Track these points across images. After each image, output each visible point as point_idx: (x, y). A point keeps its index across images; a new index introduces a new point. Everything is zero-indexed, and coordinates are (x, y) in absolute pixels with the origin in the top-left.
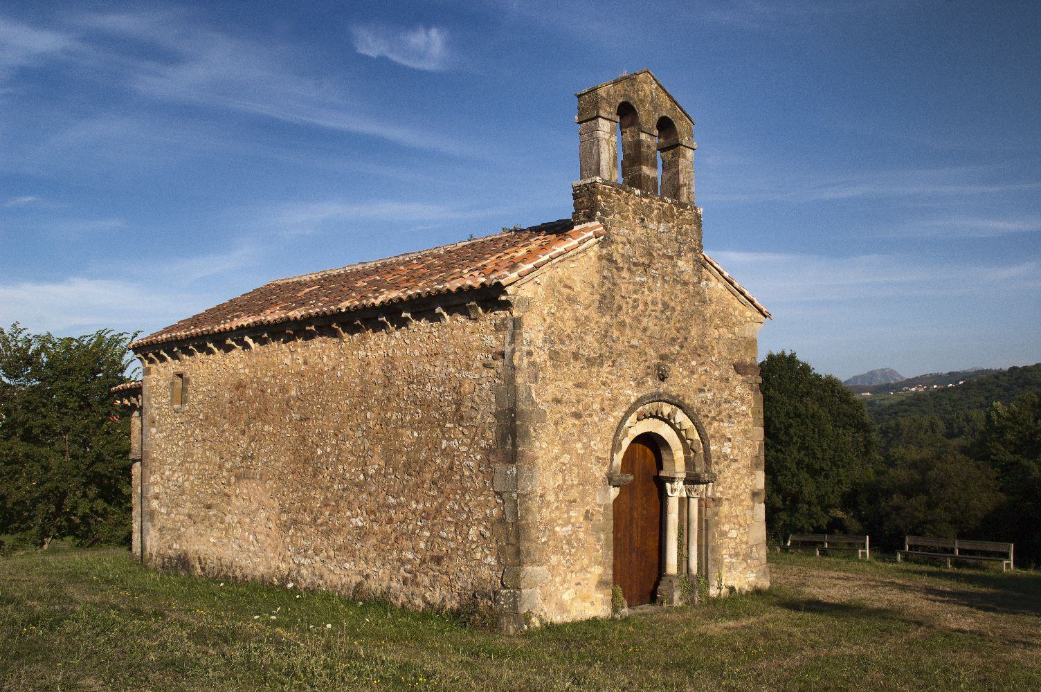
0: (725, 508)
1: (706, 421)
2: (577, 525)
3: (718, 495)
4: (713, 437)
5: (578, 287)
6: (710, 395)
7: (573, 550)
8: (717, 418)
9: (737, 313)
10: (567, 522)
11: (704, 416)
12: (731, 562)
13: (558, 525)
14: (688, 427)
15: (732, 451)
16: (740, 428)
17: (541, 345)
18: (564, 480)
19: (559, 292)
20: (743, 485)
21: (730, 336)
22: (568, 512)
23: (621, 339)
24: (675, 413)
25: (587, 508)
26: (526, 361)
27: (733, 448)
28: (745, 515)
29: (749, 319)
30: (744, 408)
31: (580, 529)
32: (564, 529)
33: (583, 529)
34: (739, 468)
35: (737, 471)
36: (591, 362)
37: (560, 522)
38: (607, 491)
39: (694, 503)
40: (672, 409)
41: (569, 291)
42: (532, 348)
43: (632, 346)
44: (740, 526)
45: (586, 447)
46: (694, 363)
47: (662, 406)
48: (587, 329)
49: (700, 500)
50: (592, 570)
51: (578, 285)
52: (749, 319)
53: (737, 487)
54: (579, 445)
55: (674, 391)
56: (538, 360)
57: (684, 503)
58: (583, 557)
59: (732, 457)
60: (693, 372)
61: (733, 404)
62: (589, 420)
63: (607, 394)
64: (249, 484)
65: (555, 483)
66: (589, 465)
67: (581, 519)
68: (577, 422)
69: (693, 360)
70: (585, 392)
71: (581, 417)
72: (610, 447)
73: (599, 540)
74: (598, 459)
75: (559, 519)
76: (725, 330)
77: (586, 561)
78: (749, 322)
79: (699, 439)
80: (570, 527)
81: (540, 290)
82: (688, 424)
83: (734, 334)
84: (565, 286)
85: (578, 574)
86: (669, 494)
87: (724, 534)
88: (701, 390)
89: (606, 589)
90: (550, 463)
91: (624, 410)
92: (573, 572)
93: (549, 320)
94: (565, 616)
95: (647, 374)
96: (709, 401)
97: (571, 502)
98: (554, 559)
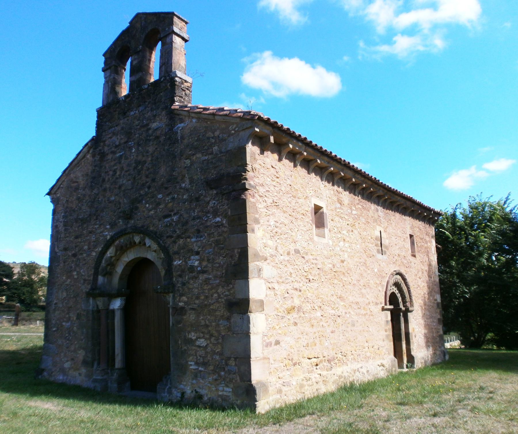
0: (191, 317)
1: (169, 241)
3: (181, 304)
6: (175, 218)
8: (183, 236)
9: (217, 133)
10: (69, 319)
11: (168, 237)
12: (198, 369)
13: (64, 321)
15: (200, 263)
16: (211, 239)
20: (216, 295)
21: (206, 158)
22: (68, 313)
24: (144, 239)
25: (78, 311)
27: (201, 260)
28: (218, 325)
29: (233, 132)
30: (218, 219)
34: (210, 279)
35: (207, 281)
36: (84, 221)
38: (88, 301)
43: (110, 202)
44: (212, 336)
45: (79, 273)
46: (160, 196)
47: (133, 237)
50: (80, 352)
52: (233, 132)
53: (207, 297)
54: (75, 273)
55: (140, 224)
59: (199, 269)
60: (159, 204)
62: (80, 257)
64: (312, 307)
68: (74, 260)
69: (160, 194)
71: (76, 256)
72: (92, 272)
74: (85, 280)
76: (199, 155)
78: (233, 134)
87: (191, 342)
88: (166, 217)
91: (102, 246)
93: (66, 205)
94: (65, 378)
95: (119, 218)
96: (174, 224)
98: (60, 342)
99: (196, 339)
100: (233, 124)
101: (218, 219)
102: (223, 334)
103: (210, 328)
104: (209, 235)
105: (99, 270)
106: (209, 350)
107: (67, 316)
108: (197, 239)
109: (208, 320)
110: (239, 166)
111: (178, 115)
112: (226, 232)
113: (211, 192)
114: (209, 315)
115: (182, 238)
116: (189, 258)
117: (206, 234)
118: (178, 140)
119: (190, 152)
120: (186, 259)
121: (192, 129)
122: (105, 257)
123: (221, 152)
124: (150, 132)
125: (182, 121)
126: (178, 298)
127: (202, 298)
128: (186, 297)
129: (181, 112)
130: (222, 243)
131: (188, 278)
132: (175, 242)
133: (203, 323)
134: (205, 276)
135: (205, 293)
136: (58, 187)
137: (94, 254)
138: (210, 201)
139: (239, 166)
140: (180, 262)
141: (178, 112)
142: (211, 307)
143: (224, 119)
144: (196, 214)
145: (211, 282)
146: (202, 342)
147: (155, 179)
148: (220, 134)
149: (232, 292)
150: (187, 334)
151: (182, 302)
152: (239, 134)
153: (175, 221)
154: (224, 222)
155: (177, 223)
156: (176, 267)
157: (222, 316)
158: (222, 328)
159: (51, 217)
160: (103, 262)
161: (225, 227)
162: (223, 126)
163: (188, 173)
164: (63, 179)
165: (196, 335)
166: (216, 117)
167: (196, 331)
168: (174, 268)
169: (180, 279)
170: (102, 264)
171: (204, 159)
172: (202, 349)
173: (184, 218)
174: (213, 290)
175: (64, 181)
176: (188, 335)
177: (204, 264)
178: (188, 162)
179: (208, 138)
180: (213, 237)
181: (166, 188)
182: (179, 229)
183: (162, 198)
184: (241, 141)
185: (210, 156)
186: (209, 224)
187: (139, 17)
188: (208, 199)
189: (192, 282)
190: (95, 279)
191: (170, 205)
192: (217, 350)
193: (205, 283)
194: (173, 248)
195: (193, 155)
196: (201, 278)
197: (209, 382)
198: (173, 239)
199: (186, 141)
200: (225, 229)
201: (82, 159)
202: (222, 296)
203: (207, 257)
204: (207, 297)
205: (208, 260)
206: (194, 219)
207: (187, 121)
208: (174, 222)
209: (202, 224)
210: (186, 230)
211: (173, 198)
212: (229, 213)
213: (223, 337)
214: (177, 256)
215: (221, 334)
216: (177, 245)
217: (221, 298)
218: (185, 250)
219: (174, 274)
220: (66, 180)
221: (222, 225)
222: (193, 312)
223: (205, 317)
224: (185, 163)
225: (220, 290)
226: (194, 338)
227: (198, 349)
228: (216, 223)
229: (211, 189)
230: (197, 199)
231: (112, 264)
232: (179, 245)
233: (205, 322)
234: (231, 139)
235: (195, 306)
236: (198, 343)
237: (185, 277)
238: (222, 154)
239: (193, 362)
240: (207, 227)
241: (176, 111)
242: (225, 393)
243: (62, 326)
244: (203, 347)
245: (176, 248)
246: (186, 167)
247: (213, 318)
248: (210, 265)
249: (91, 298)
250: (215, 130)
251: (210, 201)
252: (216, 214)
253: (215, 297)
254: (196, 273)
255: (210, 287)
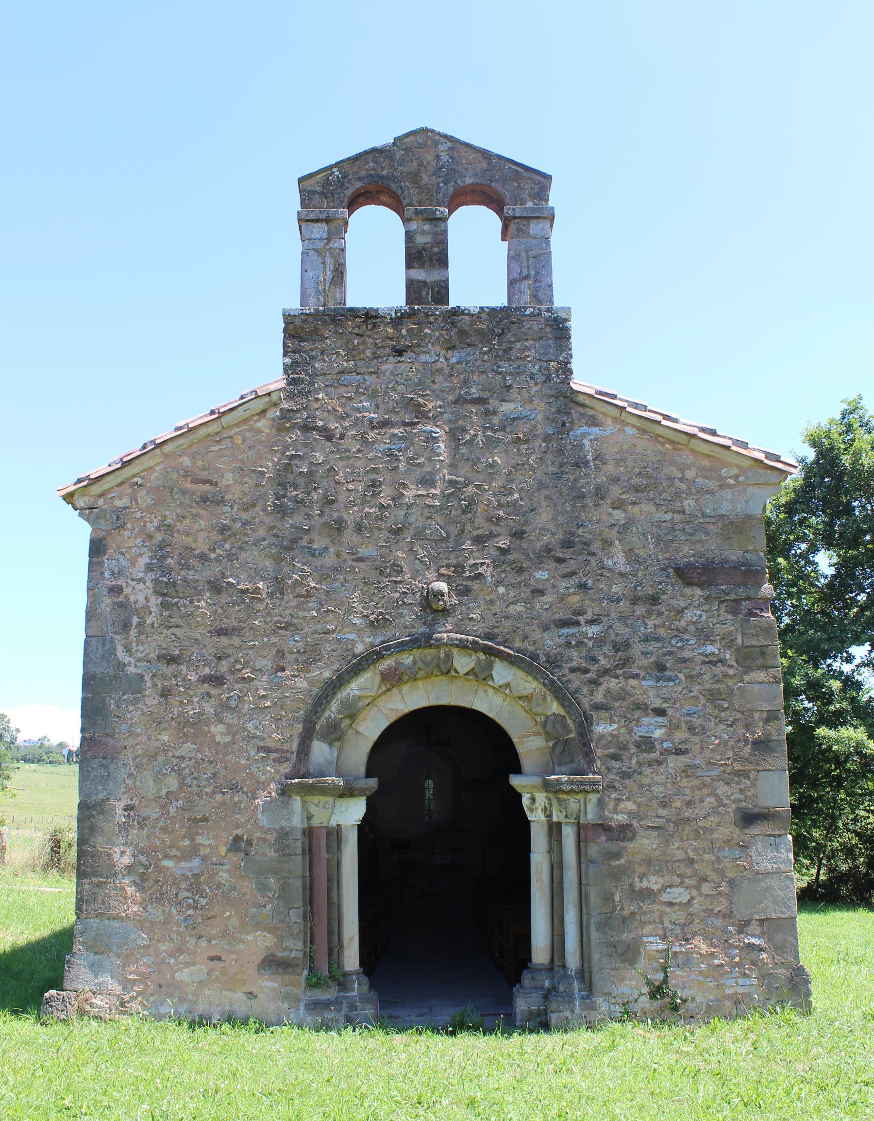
1: (576, 681)
2: (214, 859)
3: (621, 818)
4: (597, 707)
5: (229, 478)
6: (593, 630)
7: (203, 902)
8: (619, 672)
10: (193, 851)
11: (573, 670)
13: (167, 856)
14: (525, 693)
15: (669, 734)
17: (142, 575)
18: (182, 784)
19: (184, 492)
21: (669, 517)
23: (331, 550)
24: (490, 666)
25: (239, 832)
26: (107, 601)
29: (732, 482)
30: (710, 649)
31: (221, 867)
32: (183, 864)
33: (227, 867)
35: (688, 771)
37: (174, 852)
39: (569, 834)
40: (478, 658)
41: (208, 487)
42: (120, 582)
43: (360, 560)
45: (232, 731)
46: (541, 575)
48: (246, 542)
49: (580, 828)
50: (250, 938)
51: (228, 476)
52: (732, 482)
56: (132, 598)
57: (554, 830)
58: (228, 914)
59: (665, 745)
60: (539, 592)
61: (673, 642)
63: (292, 643)
65: (159, 790)
66: (243, 762)
67: (223, 850)
70: (236, 641)
73: (263, 888)
75: (171, 847)
77: (235, 921)
78: (730, 486)
79: (562, 712)
80: (196, 862)
81: (142, 493)
82: (529, 685)
83: (683, 512)
84: (196, 481)
85: (213, 942)
86: (529, 819)
87: (647, 895)
89: (285, 974)
90: (152, 757)
92: (200, 937)
93: (159, 537)
97: (196, 821)
99: (664, 888)
100: (728, 465)
101: (710, 649)
102: (730, 875)
103: (696, 866)
104: (690, 677)
105: (318, 727)
106: (696, 906)
107: (187, 843)
108: (657, 682)
109: (695, 849)
110: (747, 552)
111: (583, 406)
112: (731, 677)
113: (688, 591)
114: (695, 840)
115: (617, 677)
116: (638, 720)
117: (681, 676)
118: (587, 462)
119: (624, 497)
120: (629, 722)
121: (625, 448)
122: (339, 696)
123: (704, 515)
124: (496, 420)
125: (594, 422)
126: (612, 803)
127: (678, 804)
128: (635, 802)
129: (598, 405)
130: (724, 696)
131: (638, 763)
132: (595, 683)
133: (680, 855)
134: (683, 759)
135: (683, 795)
136: (119, 480)
137: (302, 684)
138: (687, 608)
139: (747, 552)
140: (612, 728)
141: (587, 402)
142: (701, 824)
143: (712, 451)
144: (649, 630)
145: (699, 774)
146: (680, 895)
147: (523, 532)
148: (697, 477)
149: (749, 794)
150: (637, 879)
151: (622, 813)
152: (746, 491)
153: (592, 638)
154: (728, 656)
155: (600, 641)
156: (601, 737)
157: (729, 841)
158: (729, 865)
159: (87, 559)
160: (334, 706)
161: (731, 666)
162: (706, 463)
163: (620, 540)
164: (151, 464)
165: (661, 880)
166: (693, 441)
167: (659, 873)
168: (595, 737)
169: (616, 764)
170: (327, 713)
171: (662, 519)
172: (677, 907)
173: (617, 635)
174: (704, 790)
175: (151, 469)
176: (641, 882)
177: (680, 735)
178: (619, 516)
179: (670, 479)
180: (699, 684)
181: (560, 561)
182: (606, 656)
183: (547, 580)
184: (751, 503)
185: (678, 517)
186: (686, 654)
187: (425, 130)
188: (682, 604)
189: (648, 771)
190: (304, 749)
191: (575, 599)
192: (718, 909)
193: (683, 775)
194: (592, 695)
195: (634, 503)
196: (671, 765)
197: (701, 972)
198: (588, 676)
199: (610, 468)
200: (731, 672)
201: (236, 425)
202: (726, 801)
203: (687, 722)
204: (689, 804)
205: (691, 729)
206: (646, 639)
207: (610, 428)
208: (590, 639)
209: (670, 653)
210: (626, 662)
211: (583, 586)
212: (739, 641)
213: (731, 883)
214: (603, 714)
215: (726, 877)
216: (602, 690)
217: (725, 806)
218: (625, 703)
219: (599, 752)
220: (157, 468)
221: (722, 661)
222: (654, 834)
223: (686, 843)
224: (610, 514)
225: (722, 789)
226: (655, 887)
227: (668, 910)
228: (706, 656)
229: (689, 584)
230: (654, 600)
231: (352, 712)
232: (608, 691)
233: (686, 853)
234: (727, 494)
235: (660, 822)
236: (665, 897)
237: (631, 759)
238: (708, 520)
239: (656, 936)
240: (685, 661)
241: (581, 399)
242: (740, 990)
243: (159, 868)
244: (680, 904)
245: (599, 697)
246: (614, 525)
247: (705, 845)
248: (696, 739)
249: (298, 798)
250: (689, 467)
251: (687, 608)
252: (704, 635)
253: (710, 803)
254: (658, 753)
255: (697, 782)
